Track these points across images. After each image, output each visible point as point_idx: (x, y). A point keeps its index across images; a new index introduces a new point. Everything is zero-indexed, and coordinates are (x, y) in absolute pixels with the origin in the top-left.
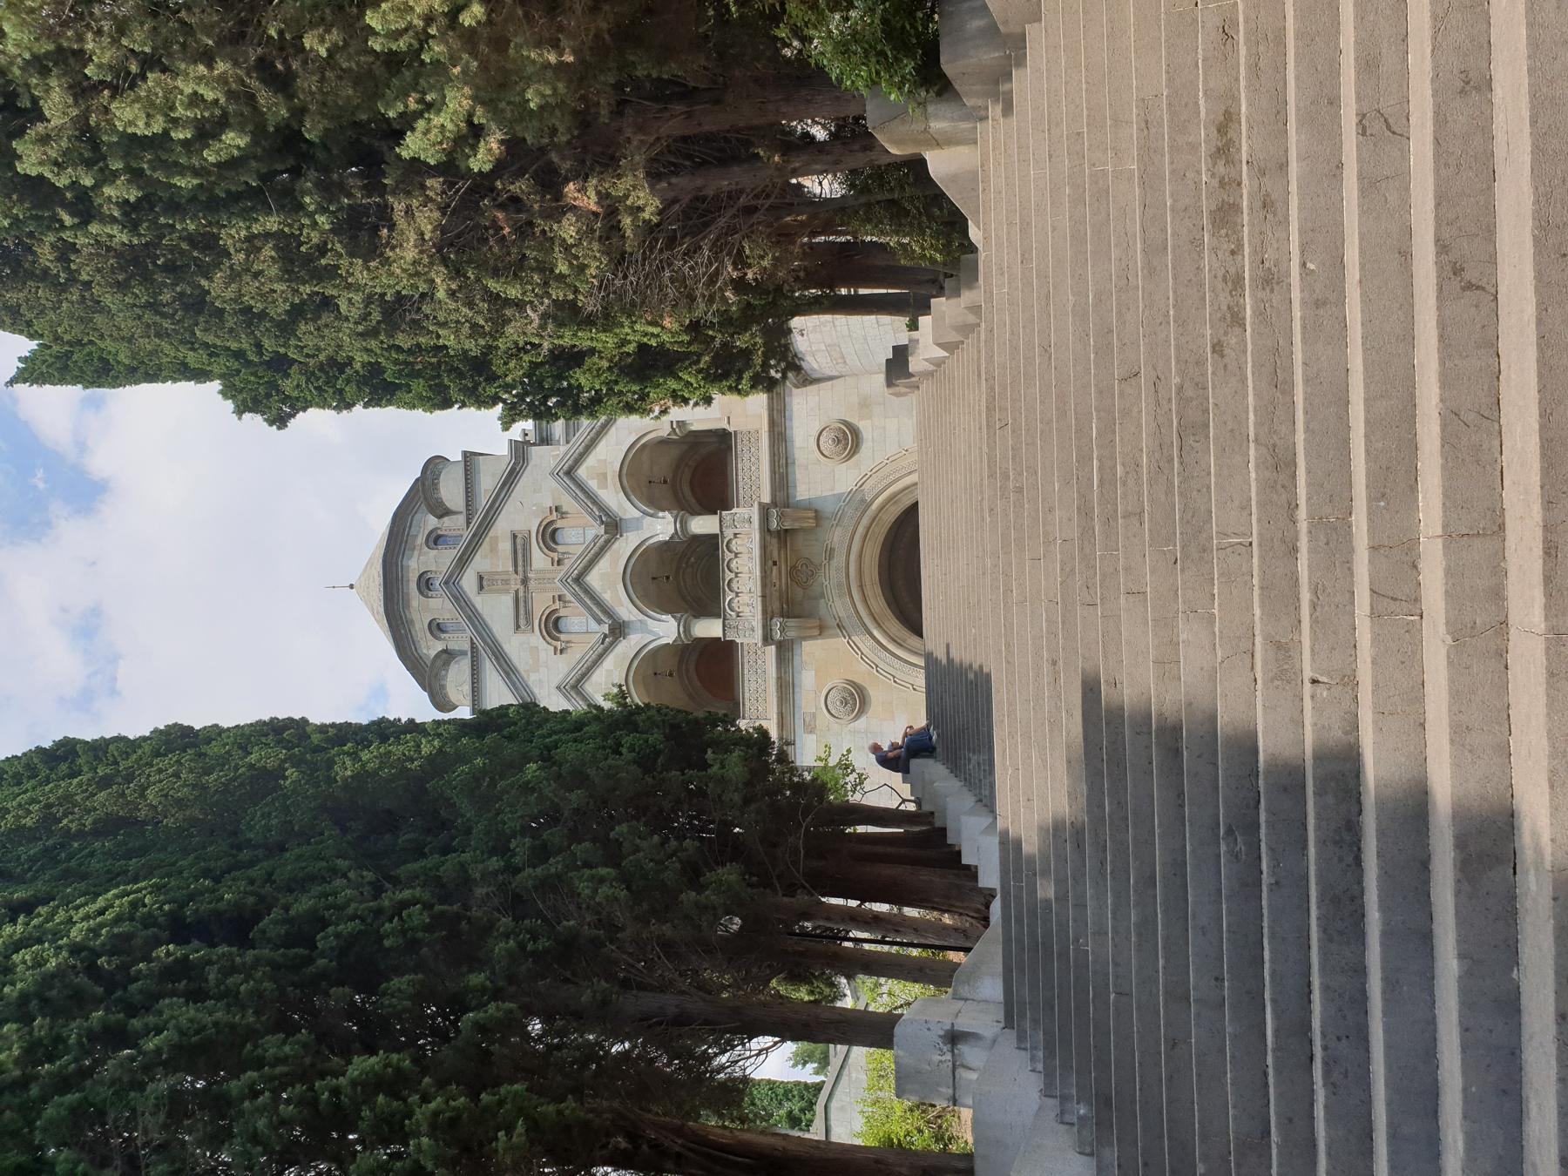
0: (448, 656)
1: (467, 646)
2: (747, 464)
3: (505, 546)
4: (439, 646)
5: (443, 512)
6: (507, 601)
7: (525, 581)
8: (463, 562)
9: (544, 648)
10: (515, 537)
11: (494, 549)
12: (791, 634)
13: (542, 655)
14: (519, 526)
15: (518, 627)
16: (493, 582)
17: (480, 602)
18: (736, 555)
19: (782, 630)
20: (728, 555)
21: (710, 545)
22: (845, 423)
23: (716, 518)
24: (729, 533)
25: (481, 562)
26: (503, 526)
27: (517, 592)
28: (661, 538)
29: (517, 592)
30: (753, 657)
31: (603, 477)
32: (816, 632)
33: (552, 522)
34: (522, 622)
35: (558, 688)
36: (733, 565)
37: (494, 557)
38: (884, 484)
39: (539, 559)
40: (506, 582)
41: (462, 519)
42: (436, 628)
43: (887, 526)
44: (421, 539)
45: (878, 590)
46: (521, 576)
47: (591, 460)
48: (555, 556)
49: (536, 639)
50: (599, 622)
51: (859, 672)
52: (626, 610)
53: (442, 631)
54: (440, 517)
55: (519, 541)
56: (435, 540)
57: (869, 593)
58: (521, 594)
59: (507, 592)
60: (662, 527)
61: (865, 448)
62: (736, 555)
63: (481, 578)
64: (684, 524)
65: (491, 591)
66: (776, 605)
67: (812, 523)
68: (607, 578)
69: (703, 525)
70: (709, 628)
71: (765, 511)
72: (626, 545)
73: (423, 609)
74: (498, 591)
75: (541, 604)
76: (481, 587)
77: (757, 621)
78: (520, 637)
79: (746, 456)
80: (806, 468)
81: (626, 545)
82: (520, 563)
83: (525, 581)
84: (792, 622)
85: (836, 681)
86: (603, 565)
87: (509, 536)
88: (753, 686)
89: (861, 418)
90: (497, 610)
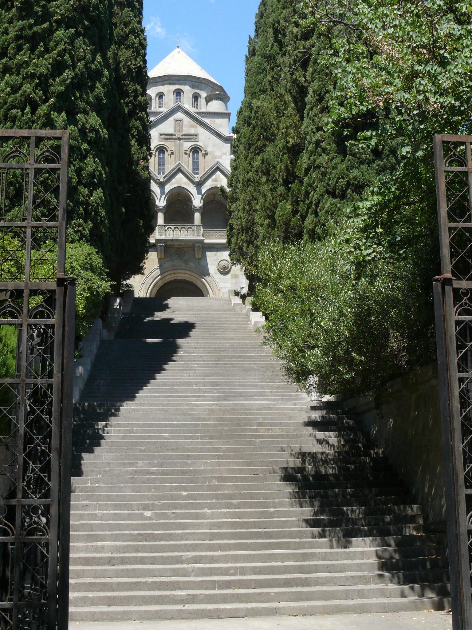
2: (218, 234)
3: (192, 131)
4: (153, 96)
5: (208, 100)
6: (171, 131)
7: (179, 139)
8: (187, 113)
10: (196, 135)
11: (192, 126)
12: (159, 248)
14: (200, 137)
15: (161, 135)
16: (179, 125)
17: (172, 119)
18: (187, 230)
19: (161, 246)
21: (190, 220)
25: (187, 120)
26: (201, 131)
27: (175, 135)
28: (193, 201)
29: (175, 135)
31: (216, 180)
32: (159, 257)
33: (201, 151)
39: (187, 145)
40: (179, 131)
41: (203, 110)
42: (160, 95)
43: (194, 282)
44: (197, 91)
45: (173, 279)
46: (181, 137)
47: (222, 176)
48: (188, 152)
50: (164, 178)
52: (168, 188)
53: (159, 98)
54: (206, 99)
55: (195, 137)
56: (196, 97)
57: (173, 275)
58: (174, 137)
59: (175, 131)
60: (197, 202)
61: (222, 276)
63: (180, 120)
64: (197, 210)
66: (168, 243)
67: (197, 257)
68: (180, 181)
70: (161, 219)
71: (201, 242)
72: (192, 189)
73: (168, 89)
75: (170, 145)
76: (177, 120)
77: (163, 237)
79: (221, 234)
80: (215, 255)
81: (192, 189)
82: (186, 137)
83: (179, 139)
87: (196, 133)
89: (232, 275)
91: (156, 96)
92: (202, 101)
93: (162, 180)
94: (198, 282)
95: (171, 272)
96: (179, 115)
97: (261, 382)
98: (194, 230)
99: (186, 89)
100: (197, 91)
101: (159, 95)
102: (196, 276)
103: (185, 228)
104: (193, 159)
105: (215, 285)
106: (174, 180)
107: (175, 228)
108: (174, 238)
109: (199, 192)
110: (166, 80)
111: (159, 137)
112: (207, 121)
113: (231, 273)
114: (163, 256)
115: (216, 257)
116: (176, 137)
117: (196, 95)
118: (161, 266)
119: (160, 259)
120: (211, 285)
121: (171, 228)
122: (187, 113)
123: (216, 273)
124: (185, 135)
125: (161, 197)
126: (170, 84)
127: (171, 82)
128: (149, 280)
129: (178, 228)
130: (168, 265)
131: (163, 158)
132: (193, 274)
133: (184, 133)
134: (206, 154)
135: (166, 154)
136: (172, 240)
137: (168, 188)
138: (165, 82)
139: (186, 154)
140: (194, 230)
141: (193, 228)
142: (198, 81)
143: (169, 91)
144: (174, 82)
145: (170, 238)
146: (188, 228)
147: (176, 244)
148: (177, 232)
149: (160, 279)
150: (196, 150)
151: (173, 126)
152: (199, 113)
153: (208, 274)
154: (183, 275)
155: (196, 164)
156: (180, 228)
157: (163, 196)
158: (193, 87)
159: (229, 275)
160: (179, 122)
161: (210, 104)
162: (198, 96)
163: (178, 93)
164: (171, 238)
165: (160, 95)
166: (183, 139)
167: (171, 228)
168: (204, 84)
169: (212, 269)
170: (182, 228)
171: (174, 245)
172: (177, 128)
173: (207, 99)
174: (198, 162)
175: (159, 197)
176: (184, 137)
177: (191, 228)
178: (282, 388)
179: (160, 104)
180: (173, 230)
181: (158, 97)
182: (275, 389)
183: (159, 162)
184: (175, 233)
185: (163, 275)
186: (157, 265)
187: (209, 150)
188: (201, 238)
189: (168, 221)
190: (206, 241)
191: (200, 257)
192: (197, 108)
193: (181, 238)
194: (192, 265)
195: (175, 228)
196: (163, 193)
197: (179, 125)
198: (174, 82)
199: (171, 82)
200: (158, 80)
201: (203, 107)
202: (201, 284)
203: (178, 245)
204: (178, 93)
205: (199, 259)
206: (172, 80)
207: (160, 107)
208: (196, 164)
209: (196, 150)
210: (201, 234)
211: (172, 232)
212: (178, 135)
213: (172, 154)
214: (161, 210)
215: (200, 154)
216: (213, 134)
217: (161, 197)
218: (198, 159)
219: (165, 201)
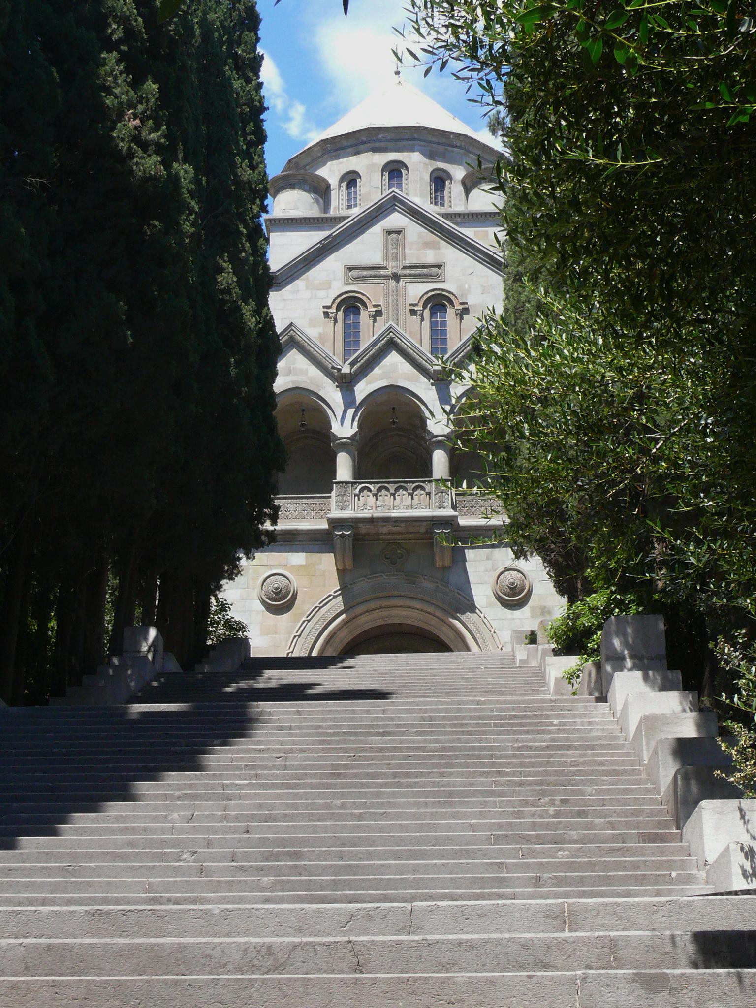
0: (321, 190)
1: (333, 212)
3: (430, 257)
4: (333, 181)
5: (468, 186)
6: (376, 258)
7: (396, 277)
8: (415, 214)
9: (328, 297)
10: (439, 266)
11: (427, 245)
13: (322, 294)
14: (449, 271)
15: (350, 269)
16: (396, 243)
18: (412, 495)
20: (410, 487)
22: (530, 592)
23: (446, 476)
24: (430, 487)
25: (414, 231)
26: (450, 255)
27: (385, 268)
29: (385, 268)
30: (318, 508)
34: (355, 273)
35: (291, 325)
36: (401, 491)
37: (419, 246)
38: (473, 629)
39: (416, 291)
40: (396, 258)
41: (458, 206)
42: (351, 179)
43: (435, 631)
45: (379, 623)
46: (401, 272)
48: (419, 308)
49: (339, 287)
50: (352, 364)
51: (303, 606)
52: (362, 390)
53: (348, 187)
56: (439, 181)
57: (376, 614)
58: (382, 272)
62: (412, 495)
63: (399, 232)
64: (440, 445)
65: (386, 242)
66: (363, 529)
67: (439, 563)
69: (440, 461)
70: (344, 467)
71: (450, 522)
73: (369, 164)
74: (386, 249)
76: (390, 232)
77: (348, 514)
78: (341, 272)
80: (488, 558)
81: (426, 391)
82: (413, 271)
83: (396, 277)
84: (349, 544)
85: (297, 582)
86: (406, 367)
87: (439, 260)
88: (291, 508)
89: (533, 609)
90: (367, 248)
91: (341, 181)
92: (455, 190)
93: (346, 369)
94: (445, 628)
95: (372, 605)
96: (396, 220)
97: (498, 839)
98: (429, 494)
99: (417, 163)
100: (441, 165)
101: (348, 178)
102: (438, 613)
103: (405, 489)
104: (433, 324)
105: (487, 635)
106: (377, 370)
107: (379, 490)
108: (378, 514)
109: (444, 397)
110: (363, 143)
111: (346, 275)
112: (469, 232)
113: (530, 603)
114: (349, 564)
115: (489, 564)
117: (440, 174)
118: (345, 589)
119: (341, 572)
120: (477, 636)
121: (369, 490)
122: (415, 214)
123: (489, 605)
124: (410, 267)
125: (345, 413)
126: (375, 150)
127: (377, 144)
128: (314, 627)
129: (387, 489)
130: (363, 585)
131: (357, 324)
132: (431, 609)
133: (408, 262)
134: (466, 311)
135: (364, 316)
136: (372, 520)
137: (362, 390)
138: (362, 147)
139: (413, 312)
140: (429, 494)
141: (428, 487)
142: (444, 140)
143: (371, 167)
144: (383, 144)
145: (366, 514)
146: (415, 489)
147: (385, 530)
148: (385, 499)
149: (345, 623)
150: (438, 303)
151: (381, 245)
152: (447, 216)
153: (472, 608)
154: (404, 612)
155: (438, 336)
156: (392, 488)
157: (351, 411)
158: (431, 156)
159: (526, 610)
160: (394, 236)
161: (475, 192)
162: (444, 176)
163: (395, 171)
164: (369, 515)
165: (351, 179)
166: (405, 276)
167: (369, 490)
168: (460, 147)
169: (482, 593)
170: (397, 489)
171: (378, 534)
172: (391, 251)
173: (469, 184)
174: (444, 332)
175: (339, 414)
176: (408, 271)
177: (423, 489)
178: (592, 866)
179: (349, 200)
180: (375, 495)
181: (344, 184)
182: (556, 867)
183: (346, 335)
184: (379, 503)
185: (352, 614)
186: (334, 585)
187: (471, 301)
188: (449, 512)
189: (360, 472)
190: (463, 521)
191: (447, 562)
192: (442, 205)
193: (395, 514)
194: (427, 585)
195: (379, 490)
196: (349, 401)
197: (396, 243)
198: (383, 144)
199: (377, 144)
200: (345, 143)
201: (457, 200)
202: (452, 635)
203: (389, 534)
204: (395, 171)
205: (445, 568)
206: (379, 141)
207: (349, 207)
208: (438, 336)
209: (438, 303)
210: (448, 503)
211: (372, 499)
212: (393, 267)
213: (379, 313)
214: (344, 447)
215: (450, 312)
216: (481, 261)
217: (345, 413)
218: (444, 324)
219: (356, 423)
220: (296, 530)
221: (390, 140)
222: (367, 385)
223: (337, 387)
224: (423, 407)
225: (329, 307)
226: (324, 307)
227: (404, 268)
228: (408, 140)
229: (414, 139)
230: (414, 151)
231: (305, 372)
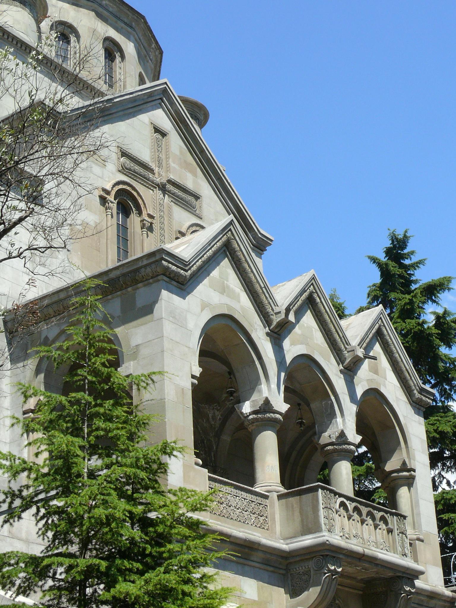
10: (197, 197)
17: (144, 119)
29: (152, 171)
40: (160, 165)
58: (151, 176)
63: (164, 134)
76: (157, 130)
82: (176, 191)
96: (160, 117)
98: (390, 531)
116: (158, 180)
126: (99, 15)
133: (172, 177)
142: (146, 45)
198: (105, 13)
199: (100, 10)
220: (259, 544)
221: (111, 13)
222: (291, 345)
223: (268, 334)
224: (333, 398)
225: (108, 193)
226: (104, 190)
227: (169, 181)
228: (125, 23)
229: (131, 27)
230: (129, 39)
231: (237, 299)
